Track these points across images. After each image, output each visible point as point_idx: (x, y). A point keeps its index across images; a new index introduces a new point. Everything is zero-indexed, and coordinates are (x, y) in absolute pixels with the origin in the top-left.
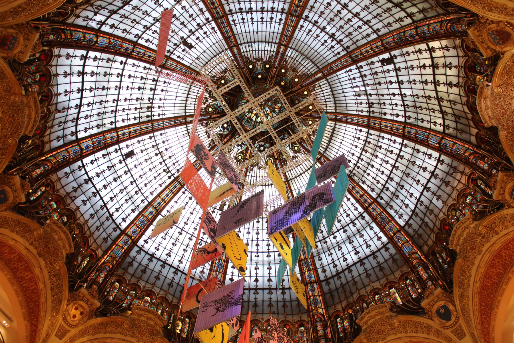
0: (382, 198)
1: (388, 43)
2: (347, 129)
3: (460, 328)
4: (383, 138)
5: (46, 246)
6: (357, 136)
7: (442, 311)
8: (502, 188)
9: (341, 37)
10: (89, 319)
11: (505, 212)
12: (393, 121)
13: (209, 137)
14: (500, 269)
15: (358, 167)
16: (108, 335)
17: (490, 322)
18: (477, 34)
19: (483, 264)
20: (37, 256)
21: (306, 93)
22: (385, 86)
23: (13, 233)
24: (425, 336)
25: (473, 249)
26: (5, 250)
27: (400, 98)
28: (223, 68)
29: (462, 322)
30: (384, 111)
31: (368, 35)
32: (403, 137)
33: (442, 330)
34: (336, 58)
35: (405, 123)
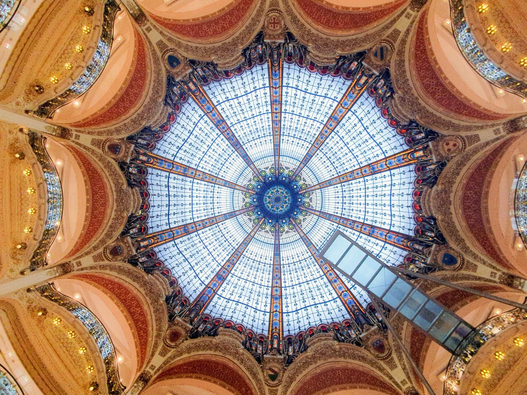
3: (161, 49)
5: (441, 205)
7: (175, 63)
8: (127, 152)
10: (446, 136)
11: (124, 135)
14: (131, 92)
16: (438, 114)
17: (139, 50)
18: (130, 252)
19: (143, 98)
20: (452, 202)
23: (459, 229)
24: (189, 44)
25: (150, 109)
26: (472, 221)
29: (160, 54)
33: (176, 48)
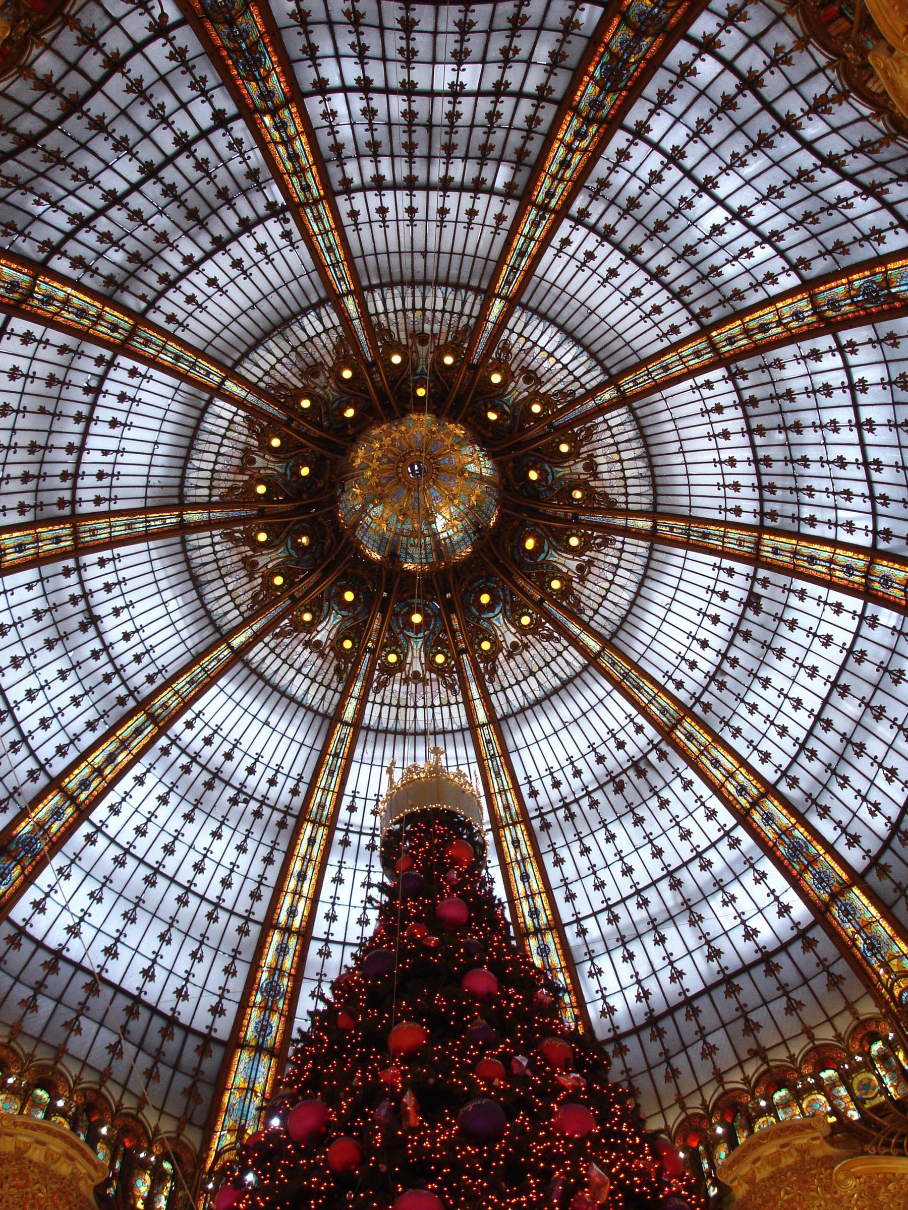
0: (582, 932)
1: (886, 581)
2: (608, 702)
4: (687, 785)
6: (621, 736)
9: (779, 482)
12: (743, 762)
13: (241, 470)
15: (571, 816)
21: (574, 542)
22: (790, 670)
27: (808, 722)
28: (427, 327)
30: (736, 722)
31: (850, 527)
32: (743, 818)
34: (721, 517)
35: (770, 790)
